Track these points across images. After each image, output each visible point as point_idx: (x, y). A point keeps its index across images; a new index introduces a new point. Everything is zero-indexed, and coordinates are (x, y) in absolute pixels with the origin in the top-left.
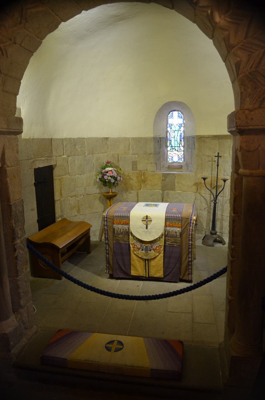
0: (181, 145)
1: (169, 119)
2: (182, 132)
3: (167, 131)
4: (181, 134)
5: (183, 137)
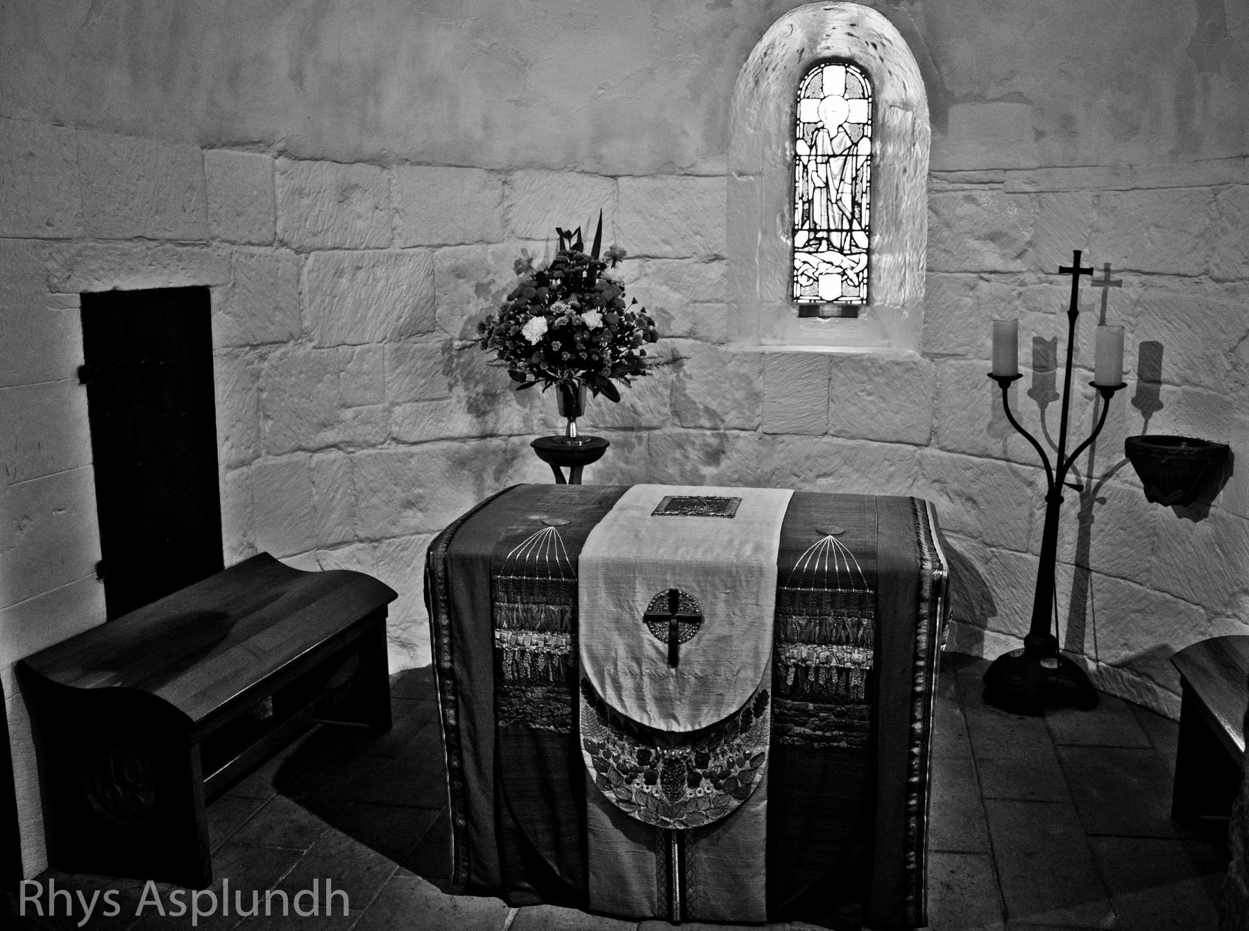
0: (856, 226)
2: (861, 160)
4: (857, 170)
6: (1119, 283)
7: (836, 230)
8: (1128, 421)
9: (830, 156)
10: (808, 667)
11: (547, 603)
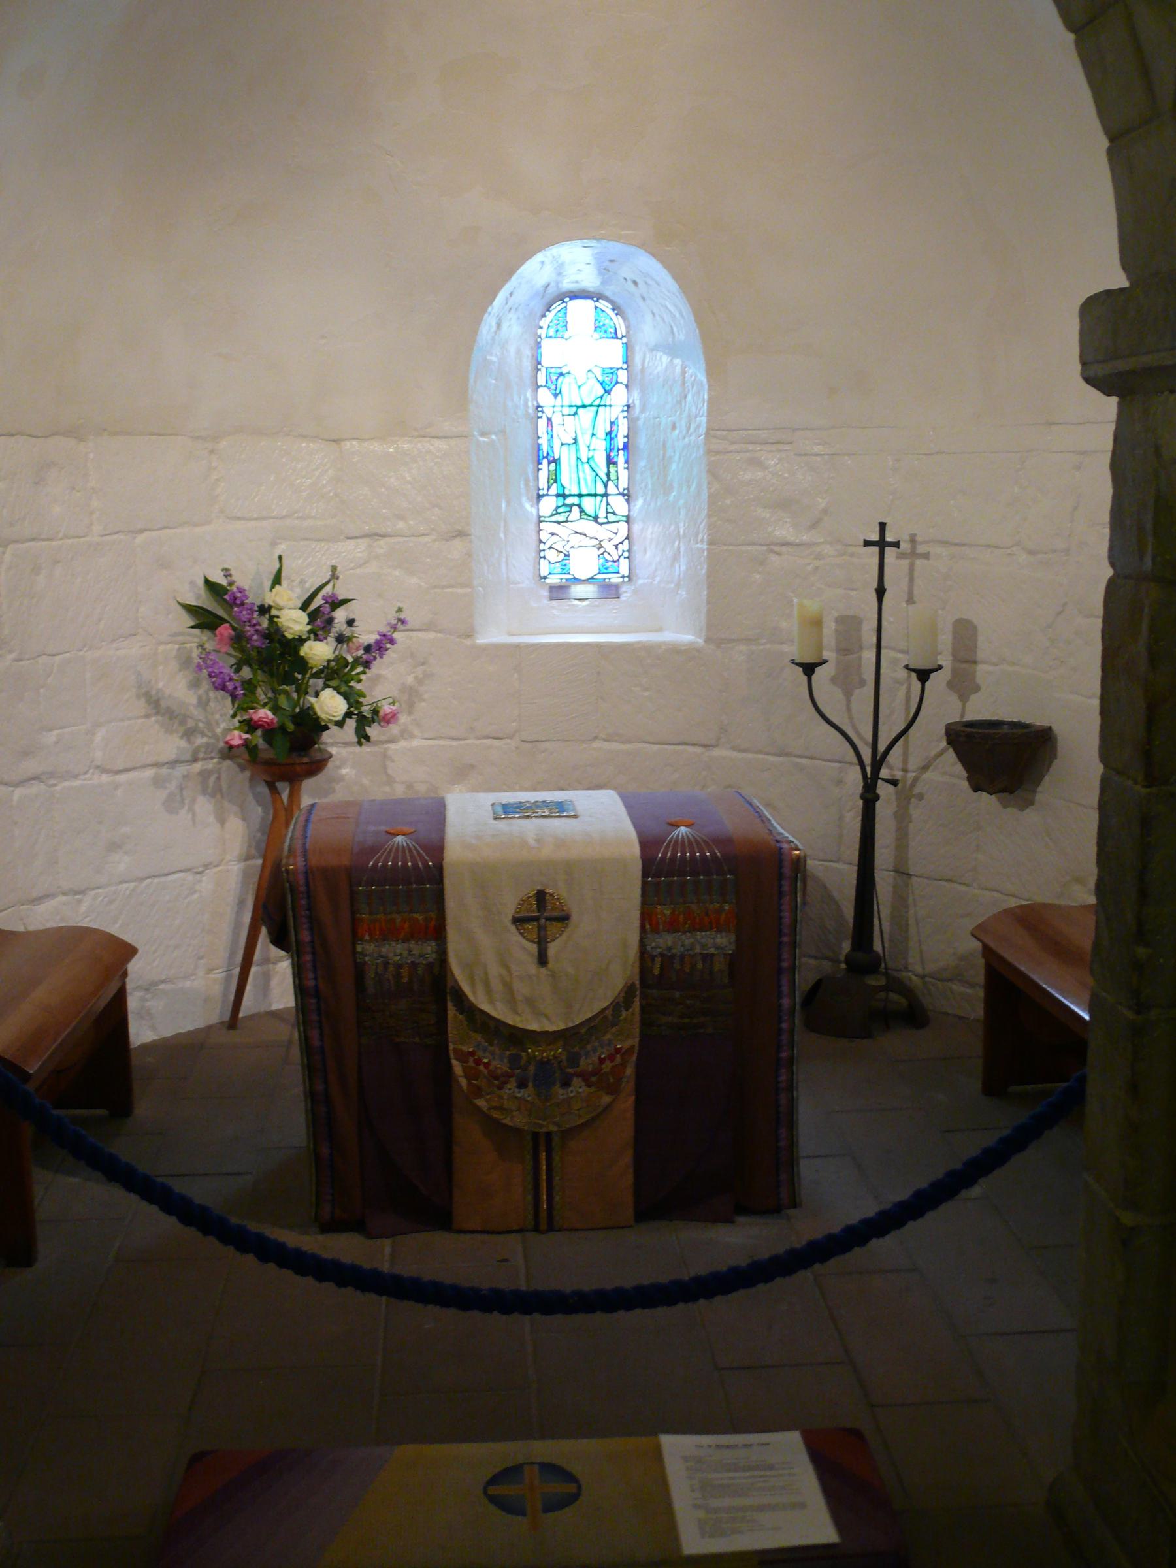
0: (611, 489)
1: (545, 343)
2: (616, 412)
4: (612, 423)
5: (620, 441)
6: (926, 556)
8: (943, 708)
9: (578, 407)
10: (674, 956)
11: (411, 912)
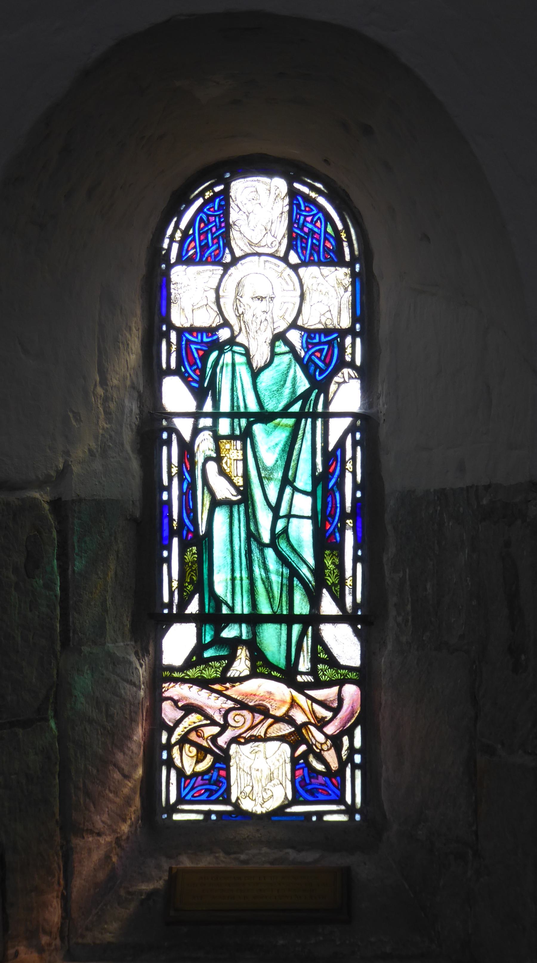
1: (179, 275)
2: (338, 427)
3: (154, 424)
7: (274, 618)
